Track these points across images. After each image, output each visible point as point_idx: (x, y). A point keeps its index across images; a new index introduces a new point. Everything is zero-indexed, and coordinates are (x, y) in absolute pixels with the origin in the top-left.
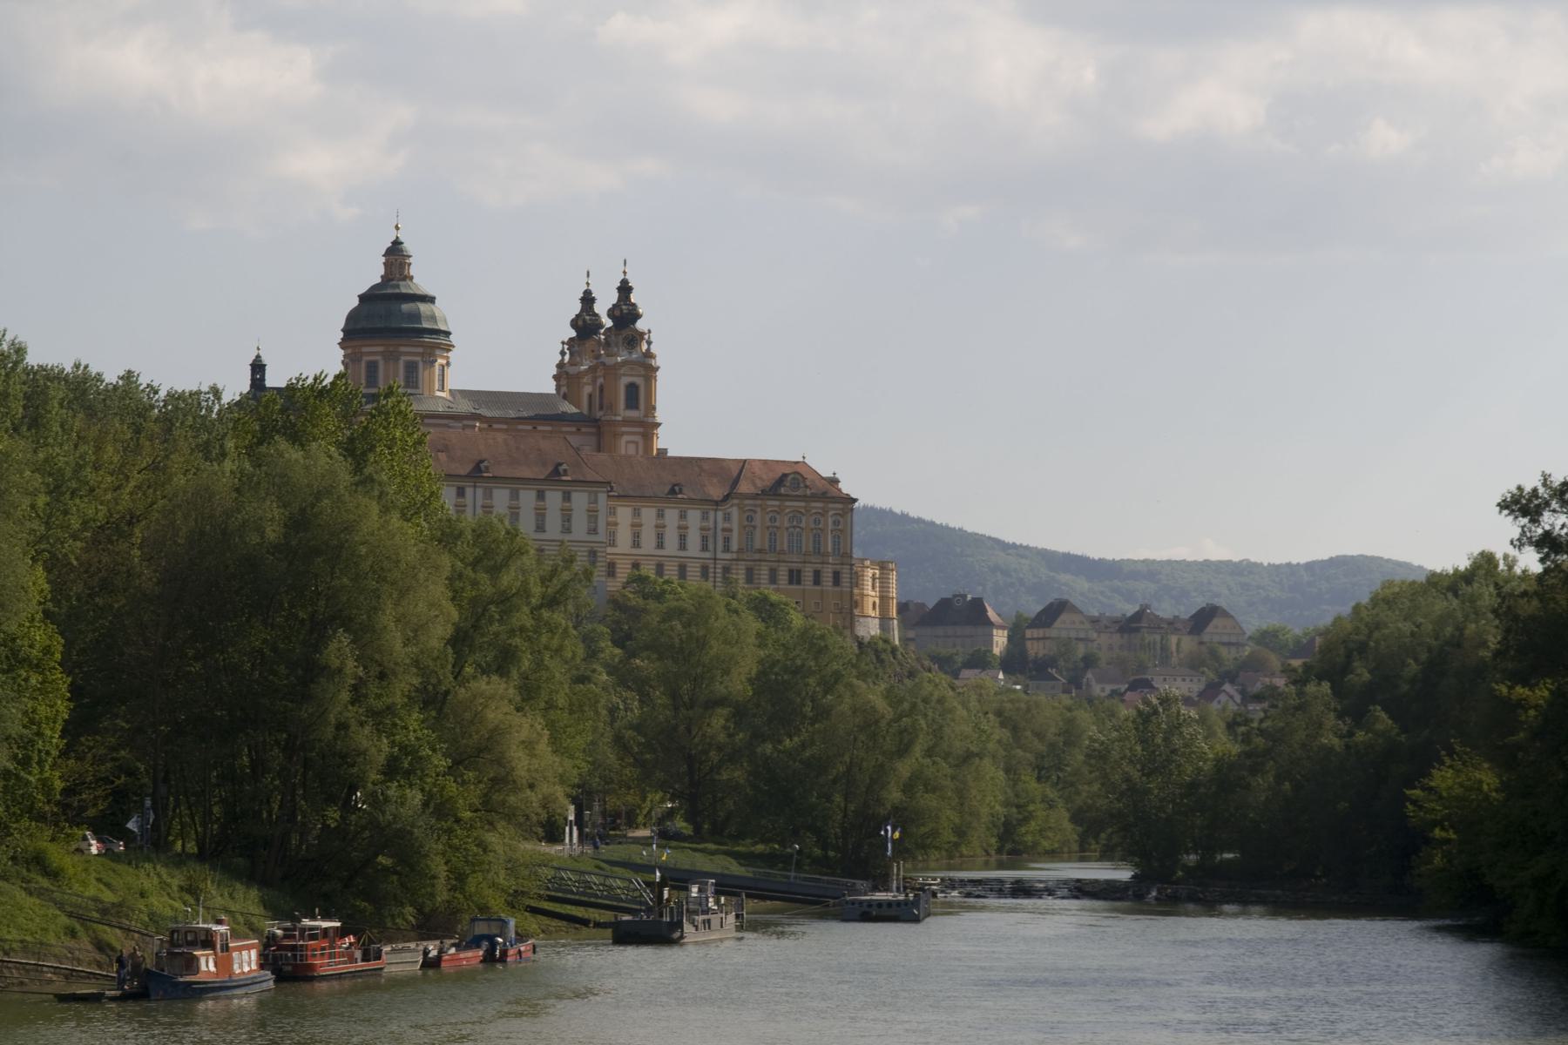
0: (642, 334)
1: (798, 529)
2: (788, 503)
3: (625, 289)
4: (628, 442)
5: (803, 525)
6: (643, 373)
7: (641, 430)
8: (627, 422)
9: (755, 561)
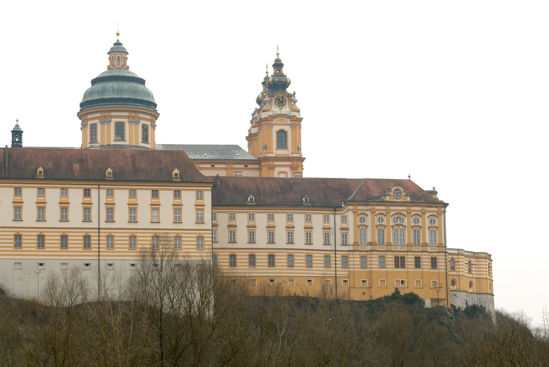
1: (401, 227)
2: (392, 208)
5: (405, 223)
6: (290, 122)
9: (367, 251)
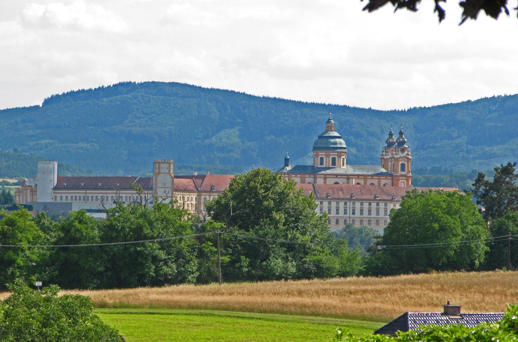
4: (401, 182)
6: (406, 160)
7: (406, 178)
8: (401, 176)
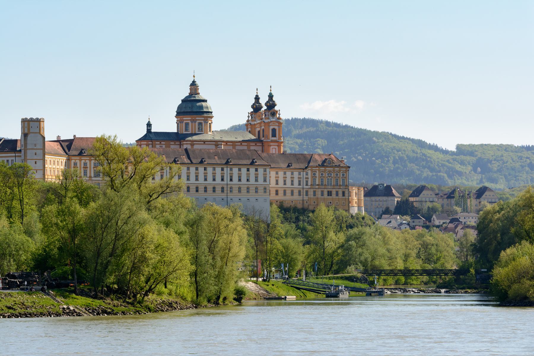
0: (277, 111)
2: (327, 169)
3: (271, 96)
4: (272, 148)
6: (277, 125)
